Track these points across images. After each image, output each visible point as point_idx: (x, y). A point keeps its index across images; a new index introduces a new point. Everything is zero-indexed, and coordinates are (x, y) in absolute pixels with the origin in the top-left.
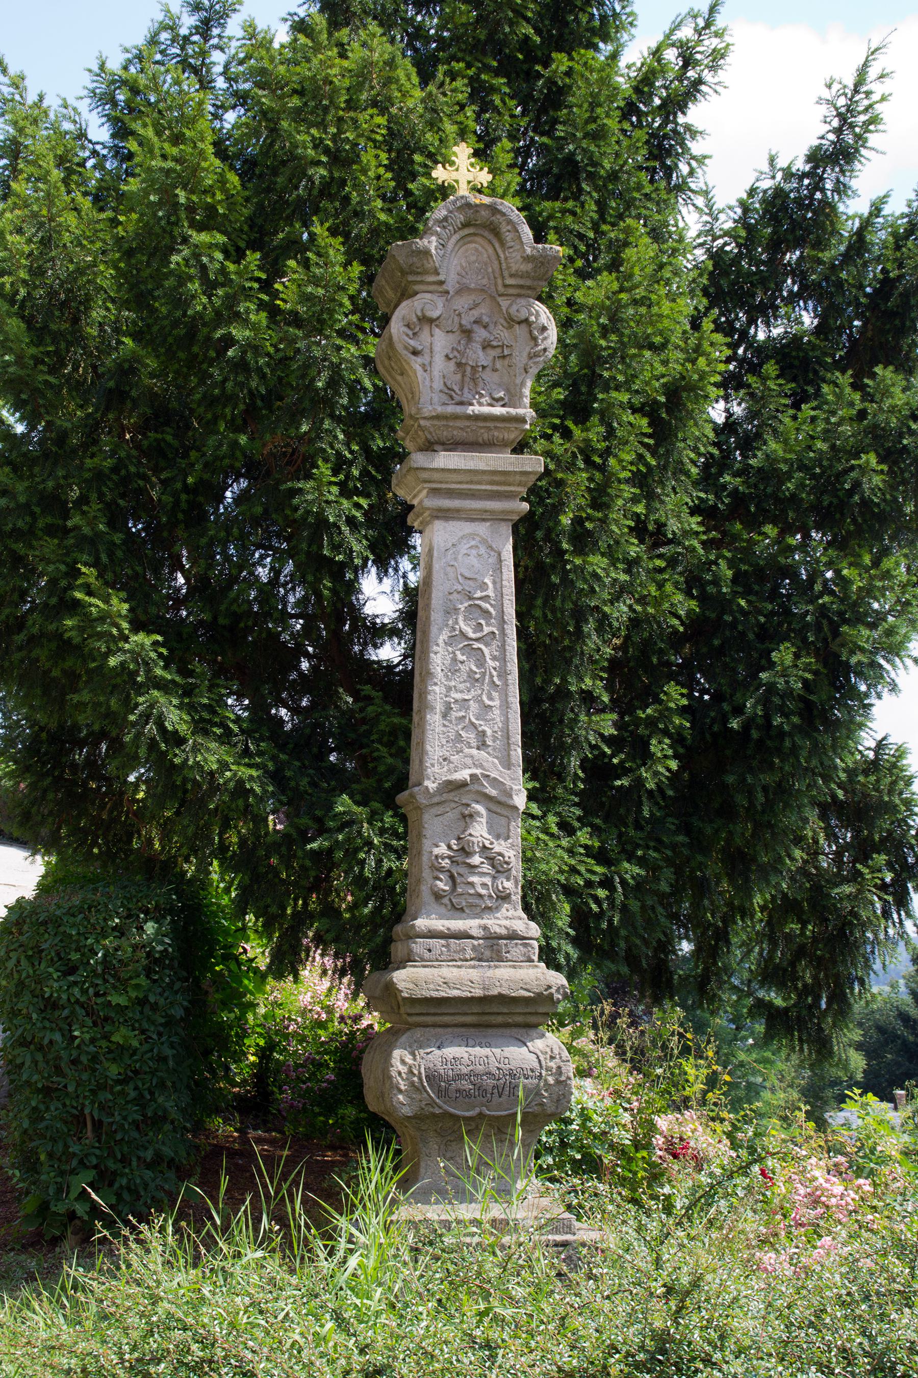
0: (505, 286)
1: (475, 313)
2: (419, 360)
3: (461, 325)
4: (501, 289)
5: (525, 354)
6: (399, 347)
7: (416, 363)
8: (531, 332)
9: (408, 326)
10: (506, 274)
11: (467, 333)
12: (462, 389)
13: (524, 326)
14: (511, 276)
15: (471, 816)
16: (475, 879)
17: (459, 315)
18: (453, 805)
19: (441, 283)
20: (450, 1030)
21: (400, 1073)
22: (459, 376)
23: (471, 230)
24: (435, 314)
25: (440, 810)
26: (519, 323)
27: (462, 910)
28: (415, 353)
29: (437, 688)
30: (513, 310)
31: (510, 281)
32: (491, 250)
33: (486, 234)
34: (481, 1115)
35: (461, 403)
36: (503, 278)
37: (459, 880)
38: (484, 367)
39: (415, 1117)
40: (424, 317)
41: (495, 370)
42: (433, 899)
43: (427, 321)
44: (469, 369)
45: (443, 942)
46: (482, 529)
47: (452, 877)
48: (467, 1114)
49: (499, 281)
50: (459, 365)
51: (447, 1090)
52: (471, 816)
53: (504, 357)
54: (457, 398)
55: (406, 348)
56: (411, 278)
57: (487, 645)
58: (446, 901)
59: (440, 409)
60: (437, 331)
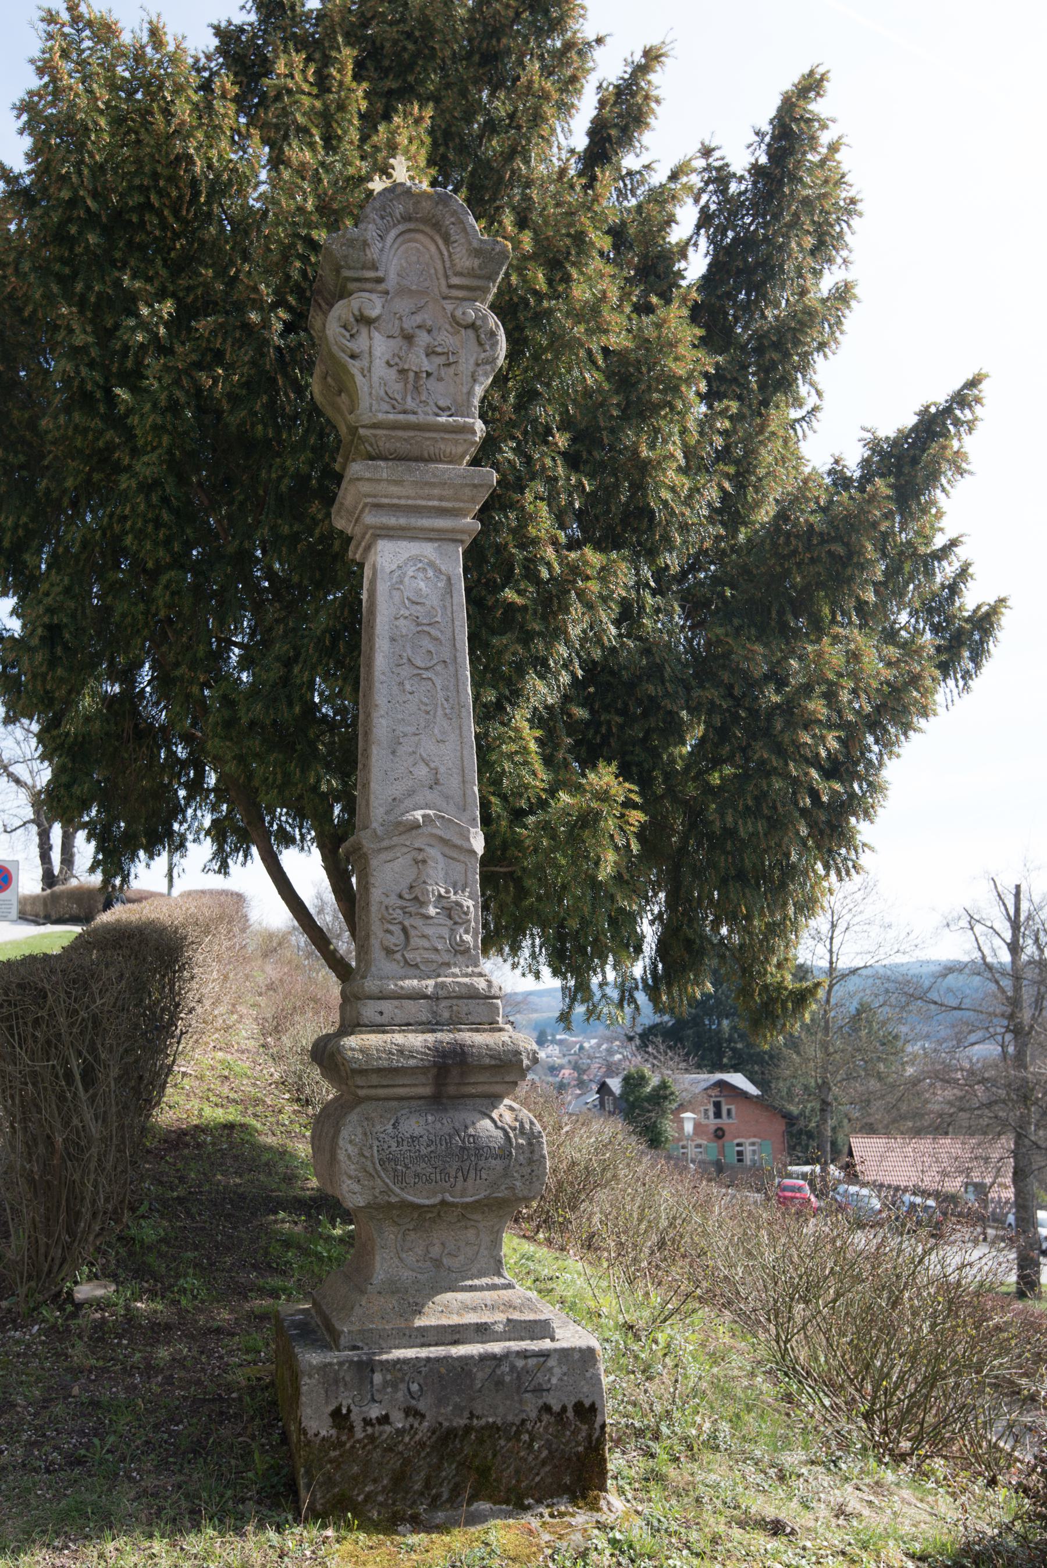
0: (450, 287)
1: (418, 319)
2: (357, 363)
3: (402, 329)
4: (445, 290)
5: (472, 361)
6: (335, 349)
7: (354, 367)
8: (478, 337)
9: (345, 327)
10: (450, 273)
11: (409, 338)
12: (404, 399)
13: (470, 333)
14: (456, 274)
15: (424, 862)
16: (429, 931)
17: (400, 319)
18: (405, 850)
19: (379, 281)
20: (405, 1103)
21: (349, 1157)
22: (402, 384)
23: (412, 226)
24: (374, 313)
25: (389, 855)
26: (466, 327)
27: (416, 966)
28: (353, 357)
29: (383, 721)
30: (458, 313)
31: (455, 281)
32: (433, 248)
33: (427, 229)
34: (443, 1203)
35: (405, 412)
36: (447, 277)
37: (412, 932)
38: (429, 374)
39: (369, 1206)
40: (361, 314)
41: (440, 379)
42: (383, 953)
43: (365, 321)
44: (411, 375)
45: (396, 1002)
46: (428, 550)
47: (404, 930)
48: (427, 1202)
49: (443, 282)
50: (402, 372)
51: (403, 1174)
52: (424, 862)
53: (449, 365)
54: (399, 407)
55: (344, 351)
56: (346, 273)
57: (437, 674)
58: (398, 956)
59: (381, 416)
60: (376, 335)
